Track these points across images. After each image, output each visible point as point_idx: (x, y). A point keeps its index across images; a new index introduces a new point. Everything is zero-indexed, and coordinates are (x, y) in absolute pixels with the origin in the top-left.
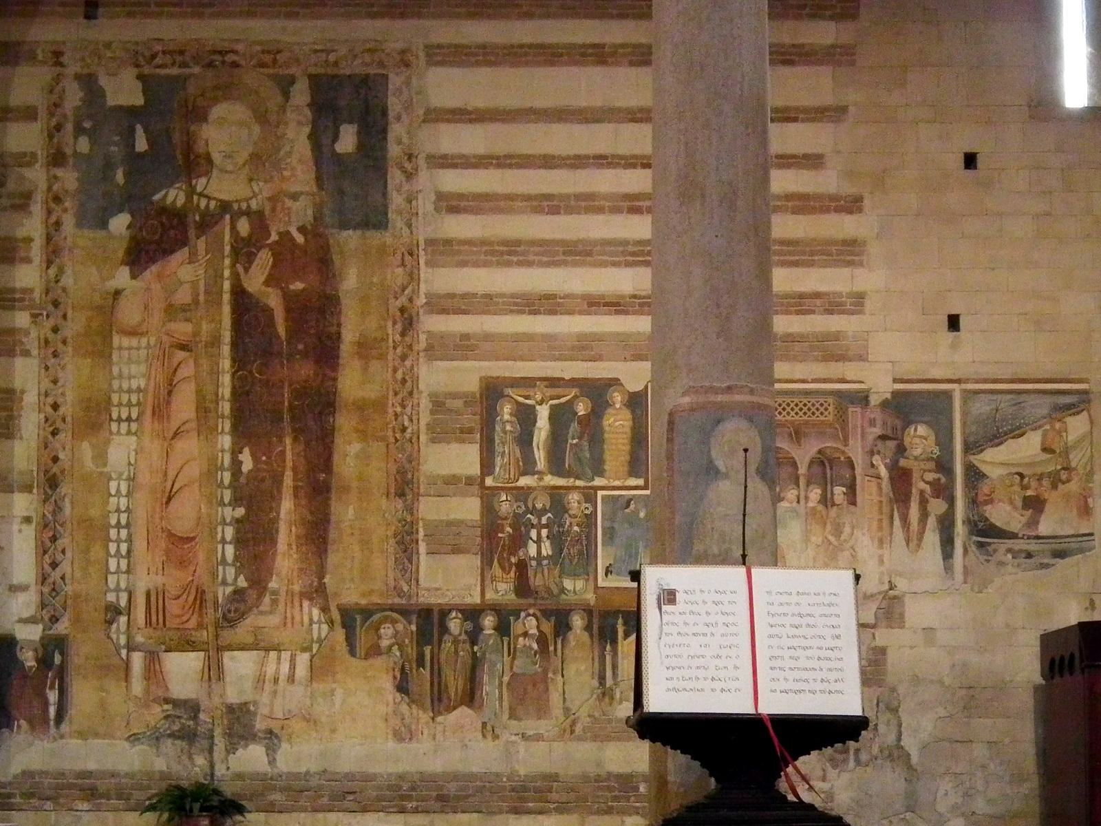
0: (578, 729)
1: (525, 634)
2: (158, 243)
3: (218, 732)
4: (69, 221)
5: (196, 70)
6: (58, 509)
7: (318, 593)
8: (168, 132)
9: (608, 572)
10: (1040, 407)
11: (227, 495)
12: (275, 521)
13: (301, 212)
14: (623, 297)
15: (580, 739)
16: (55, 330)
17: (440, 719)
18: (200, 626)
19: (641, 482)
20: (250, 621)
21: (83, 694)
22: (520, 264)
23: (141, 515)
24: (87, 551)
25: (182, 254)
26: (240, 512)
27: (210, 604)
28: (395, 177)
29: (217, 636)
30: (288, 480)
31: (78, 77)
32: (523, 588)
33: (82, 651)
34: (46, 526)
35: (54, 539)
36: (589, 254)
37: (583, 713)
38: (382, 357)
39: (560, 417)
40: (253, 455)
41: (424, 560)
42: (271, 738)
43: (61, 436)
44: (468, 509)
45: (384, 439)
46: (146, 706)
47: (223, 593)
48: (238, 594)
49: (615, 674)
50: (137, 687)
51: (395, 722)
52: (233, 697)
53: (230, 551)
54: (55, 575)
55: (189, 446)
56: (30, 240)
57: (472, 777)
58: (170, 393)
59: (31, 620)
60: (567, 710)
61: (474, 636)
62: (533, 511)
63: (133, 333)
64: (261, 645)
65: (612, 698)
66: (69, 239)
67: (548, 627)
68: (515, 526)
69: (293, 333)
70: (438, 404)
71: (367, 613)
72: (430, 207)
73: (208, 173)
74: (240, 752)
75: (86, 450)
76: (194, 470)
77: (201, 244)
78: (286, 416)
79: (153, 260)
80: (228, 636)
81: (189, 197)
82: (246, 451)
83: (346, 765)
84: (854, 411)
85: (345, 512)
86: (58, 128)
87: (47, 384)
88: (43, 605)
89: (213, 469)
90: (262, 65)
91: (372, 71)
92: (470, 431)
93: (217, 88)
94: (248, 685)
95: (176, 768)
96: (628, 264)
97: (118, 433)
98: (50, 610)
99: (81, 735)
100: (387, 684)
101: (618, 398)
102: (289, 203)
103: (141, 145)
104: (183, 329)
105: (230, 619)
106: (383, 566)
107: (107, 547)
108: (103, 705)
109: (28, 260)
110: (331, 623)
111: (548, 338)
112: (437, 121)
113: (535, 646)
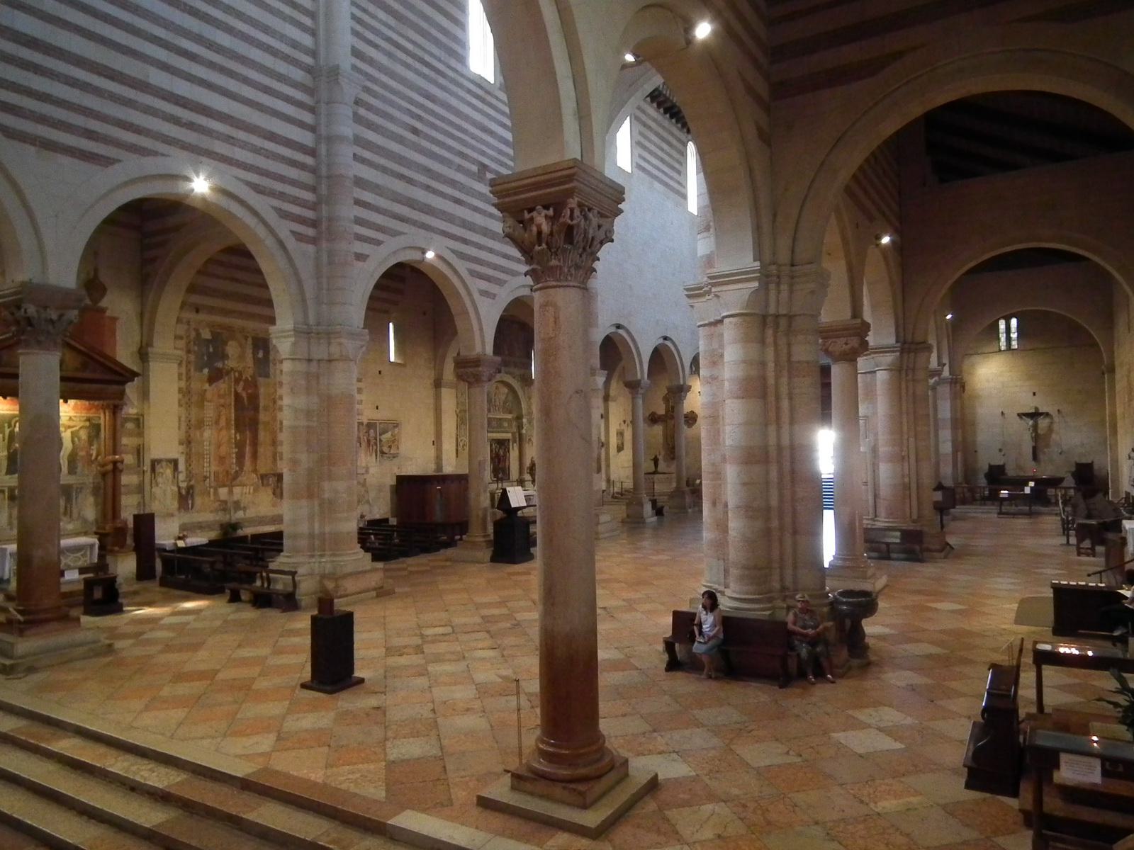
4: (192, 370)
6: (190, 450)
7: (255, 471)
10: (391, 426)
11: (234, 446)
13: (250, 372)
20: (240, 478)
21: (198, 501)
25: (222, 381)
28: (271, 365)
30: (248, 442)
31: (194, 329)
33: (197, 490)
42: (245, 509)
47: (233, 472)
48: (236, 472)
50: (212, 498)
53: (234, 461)
54: (190, 468)
55: (224, 432)
59: (184, 481)
64: (243, 485)
71: (266, 475)
77: (226, 378)
80: (234, 483)
84: (361, 426)
85: (261, 450)
86: (189, 342)
89: (230, 438)
100: (270, 491)
104: (222, 401)
105: (235, 478)
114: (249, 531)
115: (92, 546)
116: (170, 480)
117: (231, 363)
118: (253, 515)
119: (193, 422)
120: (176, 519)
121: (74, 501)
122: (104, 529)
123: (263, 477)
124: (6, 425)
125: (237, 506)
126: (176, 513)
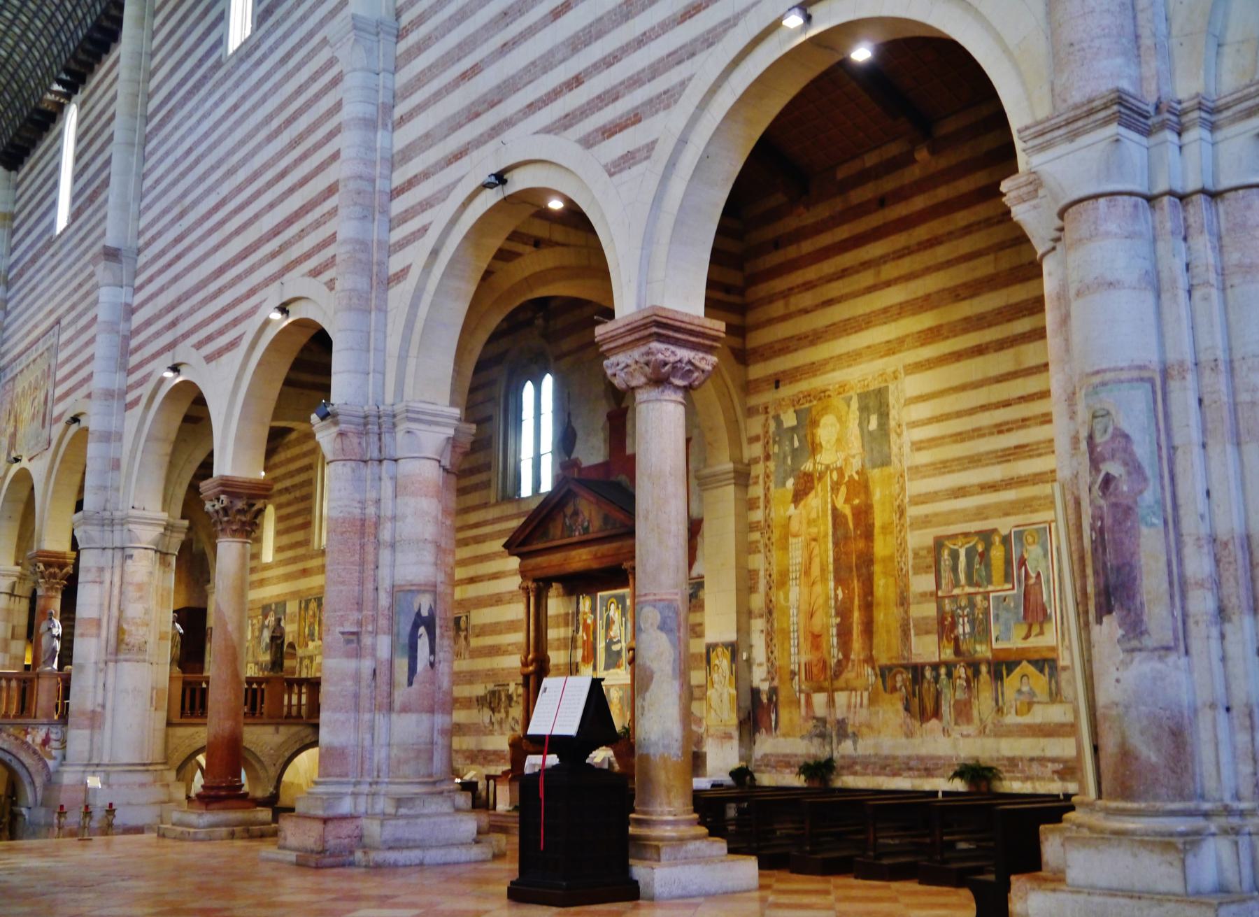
0: (987, 731)
1: (960, 677)
2: (804, 490)
3: (834, 734)
5: (815, 403)
6: (772, 627)
7: (870, 660)
8: (805, 436)
9: (997, 639)
11: (833, 612)
12: (851, 624)
13: (856, 464)
14: (996, 482)
15: (988, 736)
16: (769, 539)
17: (924, 726)
18: (825, 679)
19: (1010, 586)
21: (784, 714)
22: (949, 472)
23: (802, 626)
24: (783, 644)
25: (812, 495)
26: (838, 620)
28: (893, 437)
30: (856, 602)
31: (774, 417)
32: (957, 651)
33: (783, 694)
35: (771, 640)
36: (980, 460)
37: (989, 721)
38: (891, 533)
39: (970, 553)
40: (843, 592)
41: (913, 639)
44: (929, 610)
45: (892, 576)
47: (833, 662)
48: (839, 662)
49: (1003, 699)
51: (905, 728)
52: (839, 716)
53: (835, 640)
56: (759, 498)
57: (940, 758)
60: (981, 720)
61: (937, 679)
62: (960, 608)
63: (795, 536)
64: (849, 688)
65: (1002, 712)
67: (970, 672)
68: (952, 617)
69: (856, 526)
70: (916, 555)
72: (908, 450)
73: (821, 452)
74: (843, 744)
75: (781, 594)
76: (821, 601)
78: (854, 569)
79: (801, 499)
81: (814, 465)
82: (840, 589)
83: (885, 751)
86: (768, 443)
87: (767, 565)
88: (769, 672)
89: (827, 599)
90: (839, 393)
91: (883, 385)
92: (930, 567)
93: (823, 409)
94: (845, 709)
95: (819, 753)
96: (999, 463)
98: (771, 676)
99: (784, 736)
100: (900, 706)
101: (997, 539)
102: (851, 460)
103: (796, 444)
104: (814, 530)
105: (837, 675)
106: (896, 642)
108: (791, 720)
109: (758, 507)
110: (876, 675)
111: (964, 511)
112: (910, 404)
113: (965, 684)
114: (849, 781)
117: (826, 457)
118: (871, 752)
119: (774, 577)
123: (885, 673)
125: (842, 729)
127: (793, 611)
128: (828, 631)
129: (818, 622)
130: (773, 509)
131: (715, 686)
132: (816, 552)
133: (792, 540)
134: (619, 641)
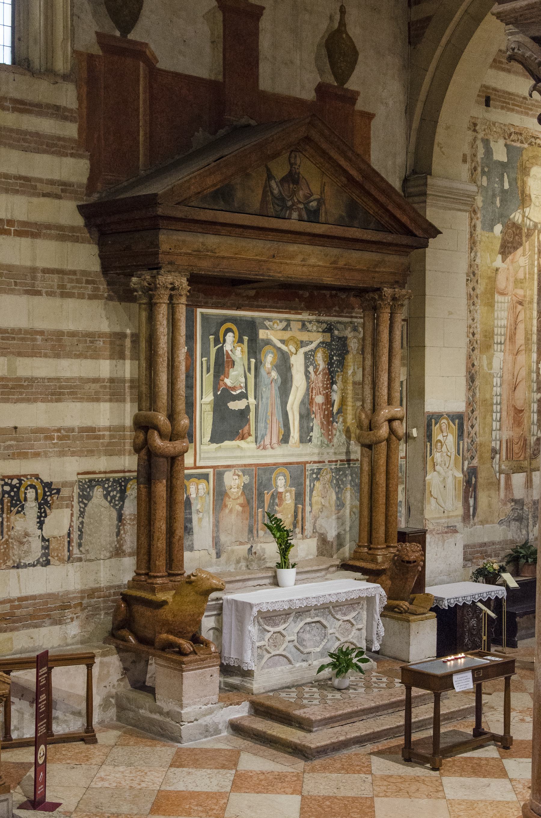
3: (530, 516)
23: (505, 397)
24: (485, 418)
25: (520, 251)
27: (528, 447)
29: (530, 464)
31: (483, 140)
33: (482, 476)
34: (470, 404)
43: (476, 352)
46: (505, 504)
58: (515, 328)
63: (502, 294)
66: (479, 236)
79: (510, 253)
86: (475, 169)
89: (530, 372)
95: (516, 537)
97: (497, 351)
99: (482, 523)
103: (506, 186)
107: (492, 416)
108: (490, 506)
115: (370, 600)
116: (453, 457)
120: (459, 536)
121: (307, 499)
122: (374, 560)
124: (212, 337)
126: (460, 525)
127: (496, 381)
128: (530, 406)
129: (521, 394)
130: (479, 254)
131: (438, 468)
132: (521, 317)
133: (498, 298)
134: (244, 396)
